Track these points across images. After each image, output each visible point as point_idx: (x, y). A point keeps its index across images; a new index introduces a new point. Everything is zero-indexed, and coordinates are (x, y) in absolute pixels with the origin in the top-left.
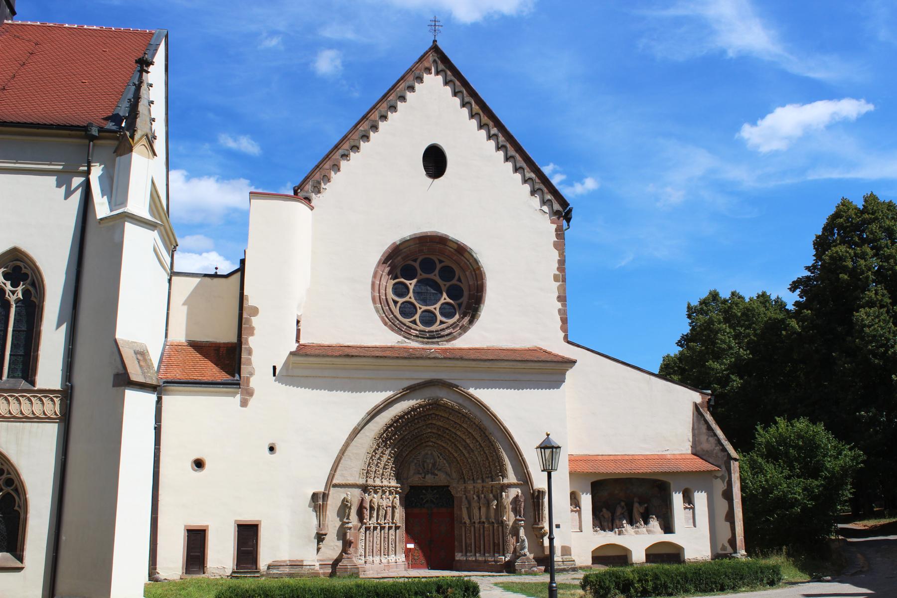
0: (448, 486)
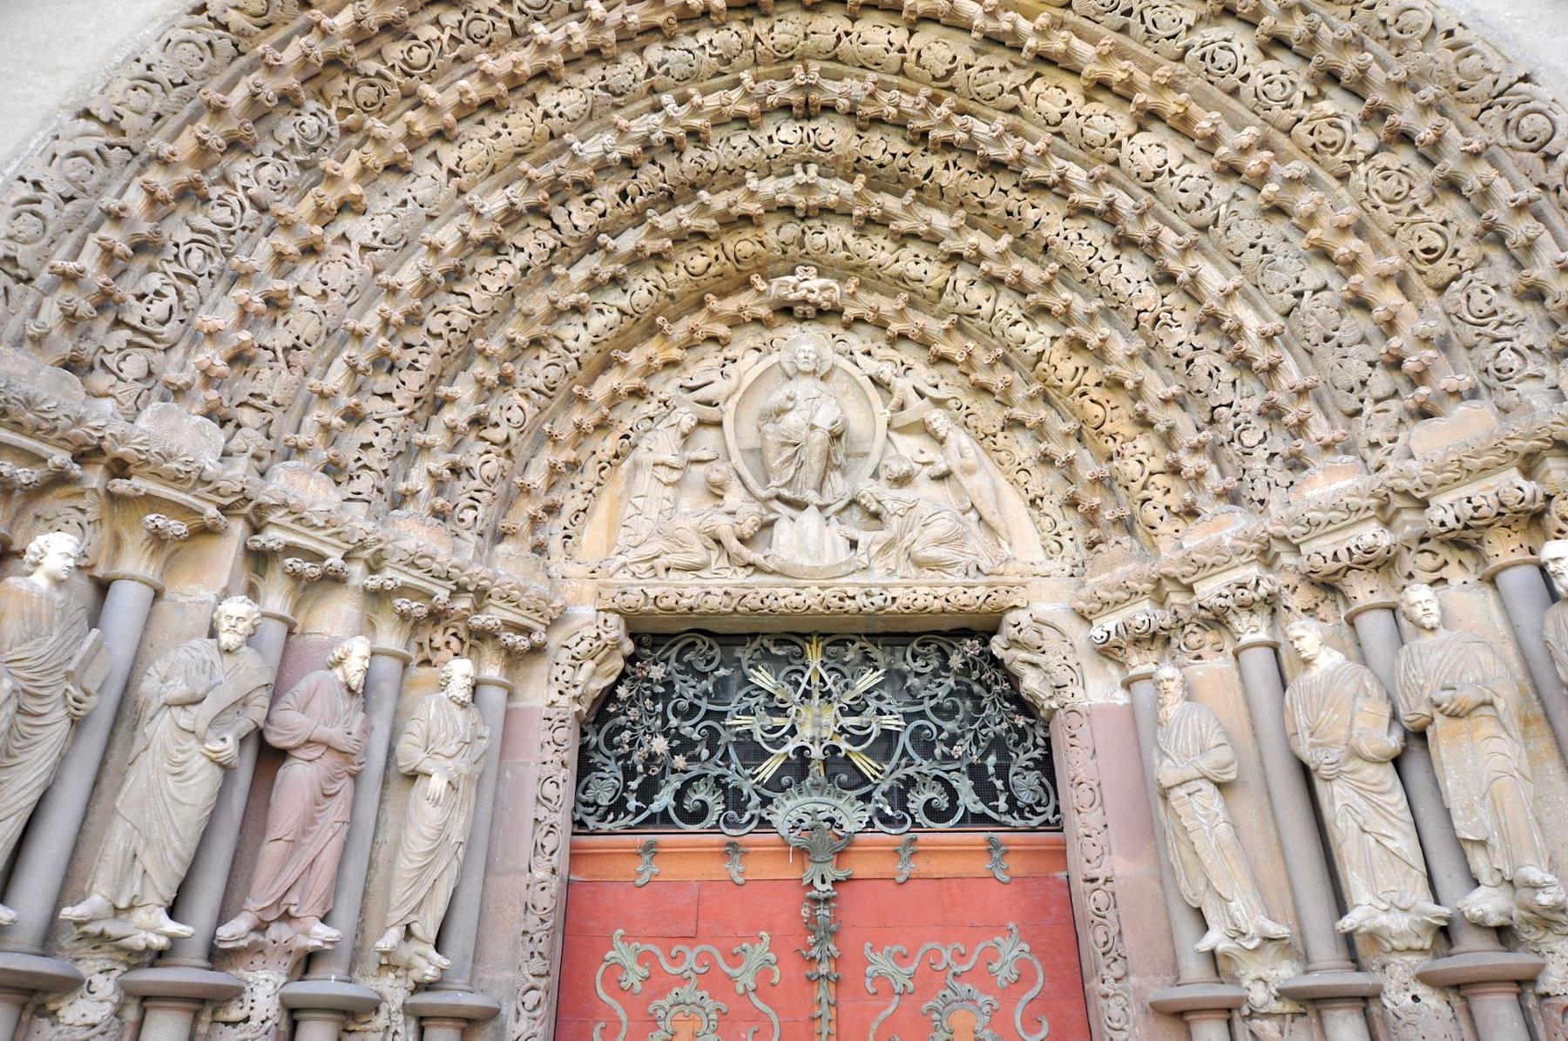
0: (983, 626)
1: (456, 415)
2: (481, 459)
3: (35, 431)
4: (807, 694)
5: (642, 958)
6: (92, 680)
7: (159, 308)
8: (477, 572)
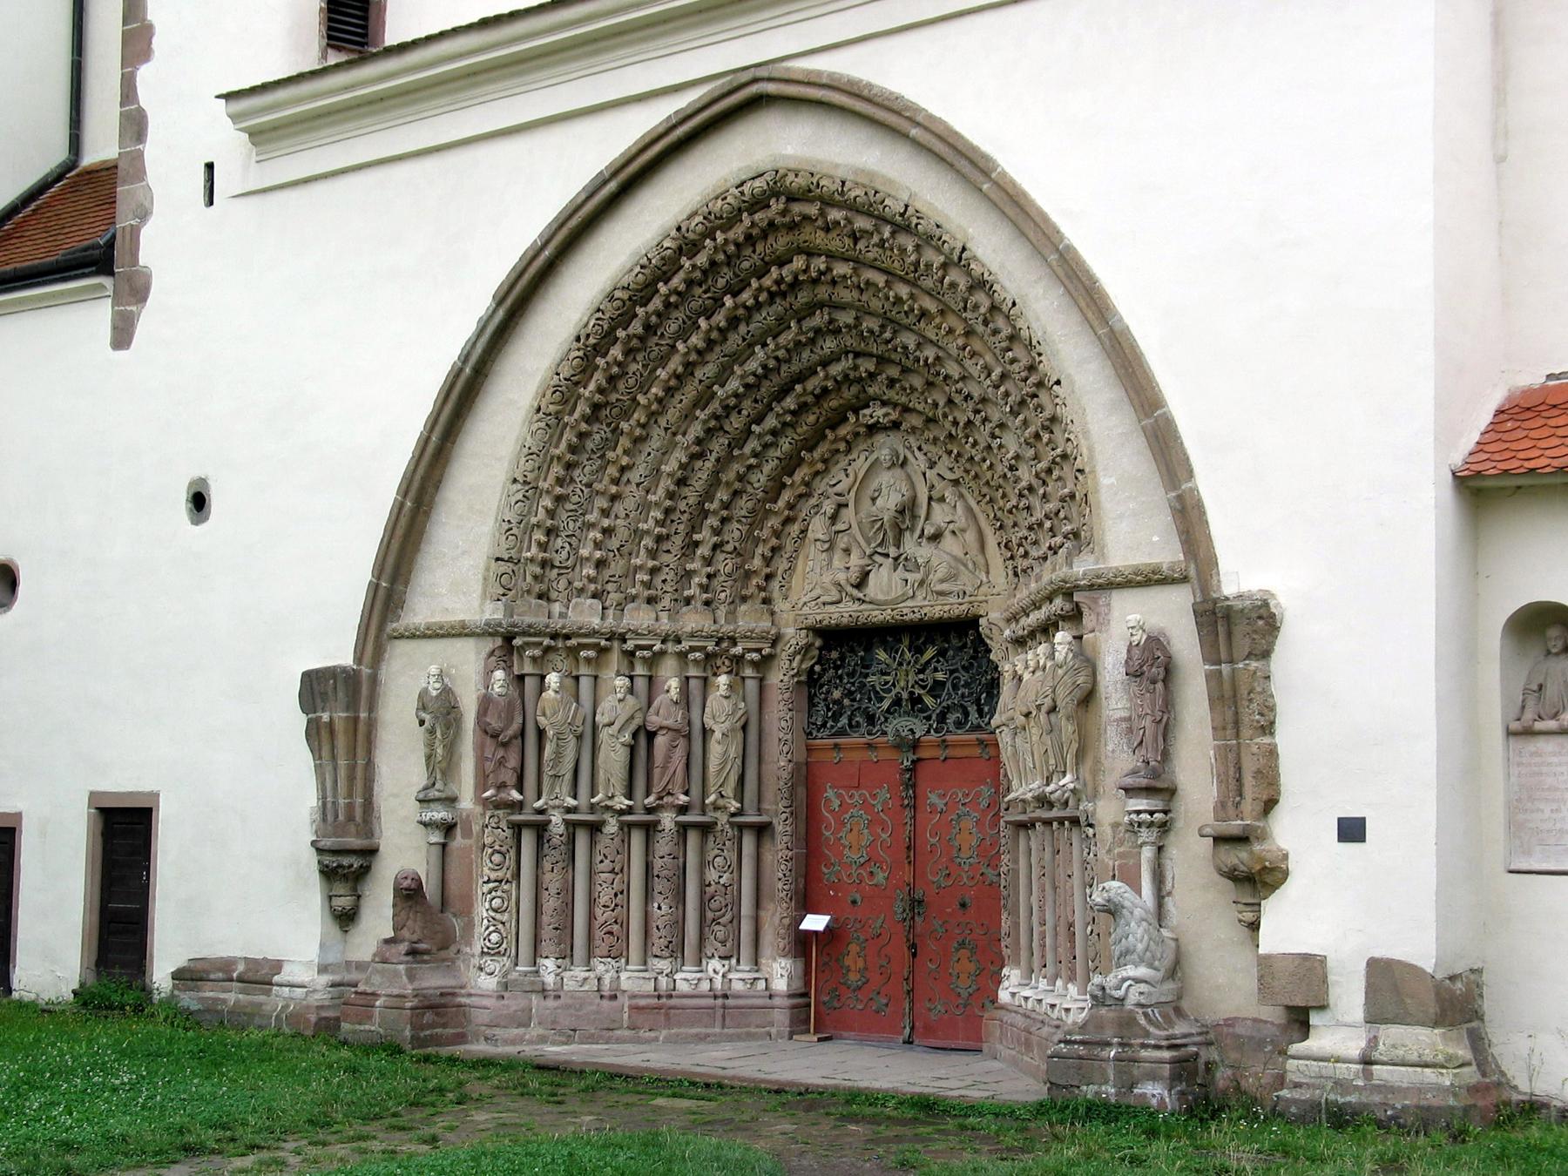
0: (971, 623)
1: (704, 550)
2: (724, 564)
3: (535, 635)
4: (900, 664)
5: (839, 796)
6: (579, 721)
7: (564, 554)
8: (727, 629)
